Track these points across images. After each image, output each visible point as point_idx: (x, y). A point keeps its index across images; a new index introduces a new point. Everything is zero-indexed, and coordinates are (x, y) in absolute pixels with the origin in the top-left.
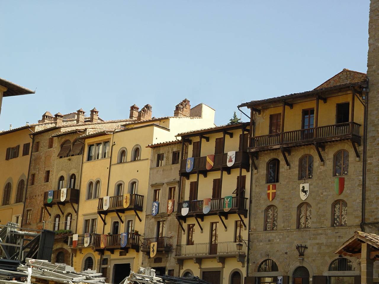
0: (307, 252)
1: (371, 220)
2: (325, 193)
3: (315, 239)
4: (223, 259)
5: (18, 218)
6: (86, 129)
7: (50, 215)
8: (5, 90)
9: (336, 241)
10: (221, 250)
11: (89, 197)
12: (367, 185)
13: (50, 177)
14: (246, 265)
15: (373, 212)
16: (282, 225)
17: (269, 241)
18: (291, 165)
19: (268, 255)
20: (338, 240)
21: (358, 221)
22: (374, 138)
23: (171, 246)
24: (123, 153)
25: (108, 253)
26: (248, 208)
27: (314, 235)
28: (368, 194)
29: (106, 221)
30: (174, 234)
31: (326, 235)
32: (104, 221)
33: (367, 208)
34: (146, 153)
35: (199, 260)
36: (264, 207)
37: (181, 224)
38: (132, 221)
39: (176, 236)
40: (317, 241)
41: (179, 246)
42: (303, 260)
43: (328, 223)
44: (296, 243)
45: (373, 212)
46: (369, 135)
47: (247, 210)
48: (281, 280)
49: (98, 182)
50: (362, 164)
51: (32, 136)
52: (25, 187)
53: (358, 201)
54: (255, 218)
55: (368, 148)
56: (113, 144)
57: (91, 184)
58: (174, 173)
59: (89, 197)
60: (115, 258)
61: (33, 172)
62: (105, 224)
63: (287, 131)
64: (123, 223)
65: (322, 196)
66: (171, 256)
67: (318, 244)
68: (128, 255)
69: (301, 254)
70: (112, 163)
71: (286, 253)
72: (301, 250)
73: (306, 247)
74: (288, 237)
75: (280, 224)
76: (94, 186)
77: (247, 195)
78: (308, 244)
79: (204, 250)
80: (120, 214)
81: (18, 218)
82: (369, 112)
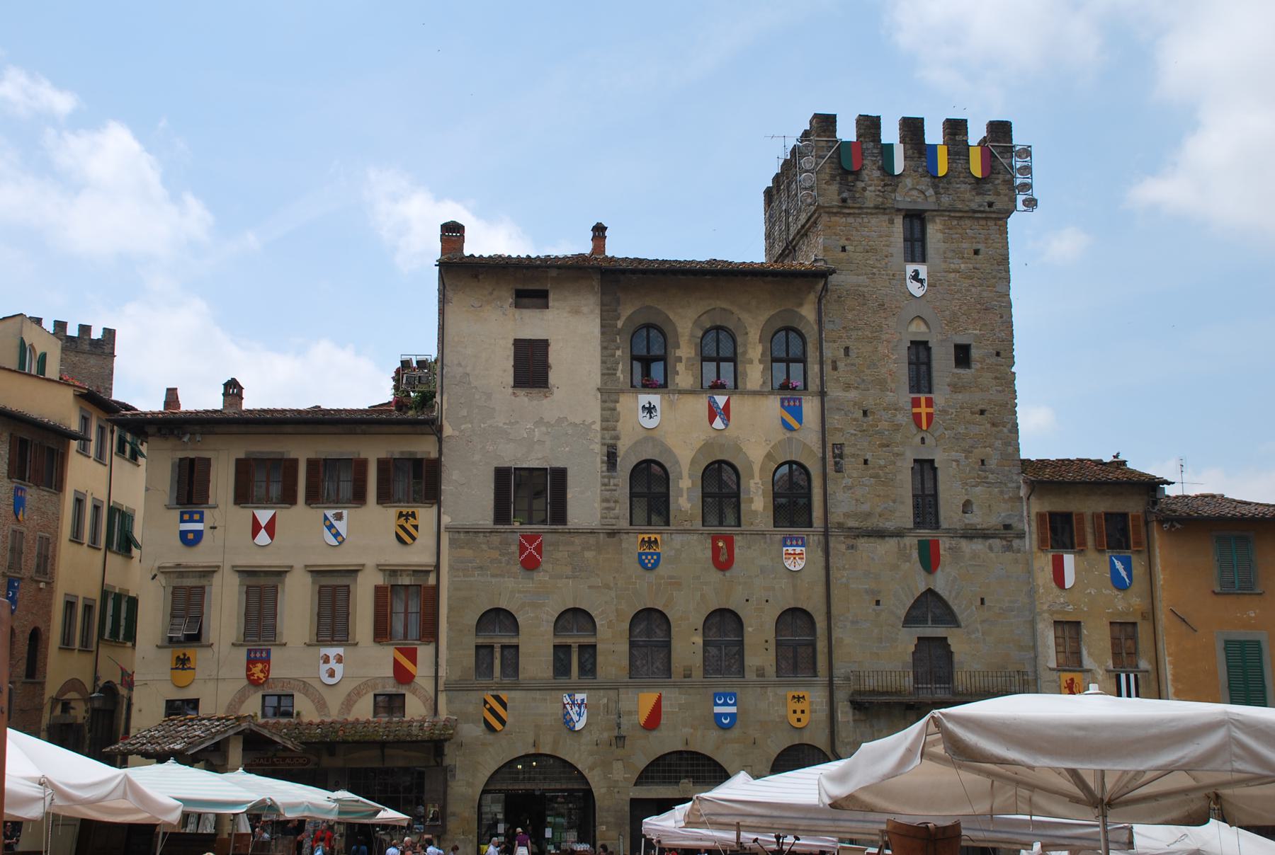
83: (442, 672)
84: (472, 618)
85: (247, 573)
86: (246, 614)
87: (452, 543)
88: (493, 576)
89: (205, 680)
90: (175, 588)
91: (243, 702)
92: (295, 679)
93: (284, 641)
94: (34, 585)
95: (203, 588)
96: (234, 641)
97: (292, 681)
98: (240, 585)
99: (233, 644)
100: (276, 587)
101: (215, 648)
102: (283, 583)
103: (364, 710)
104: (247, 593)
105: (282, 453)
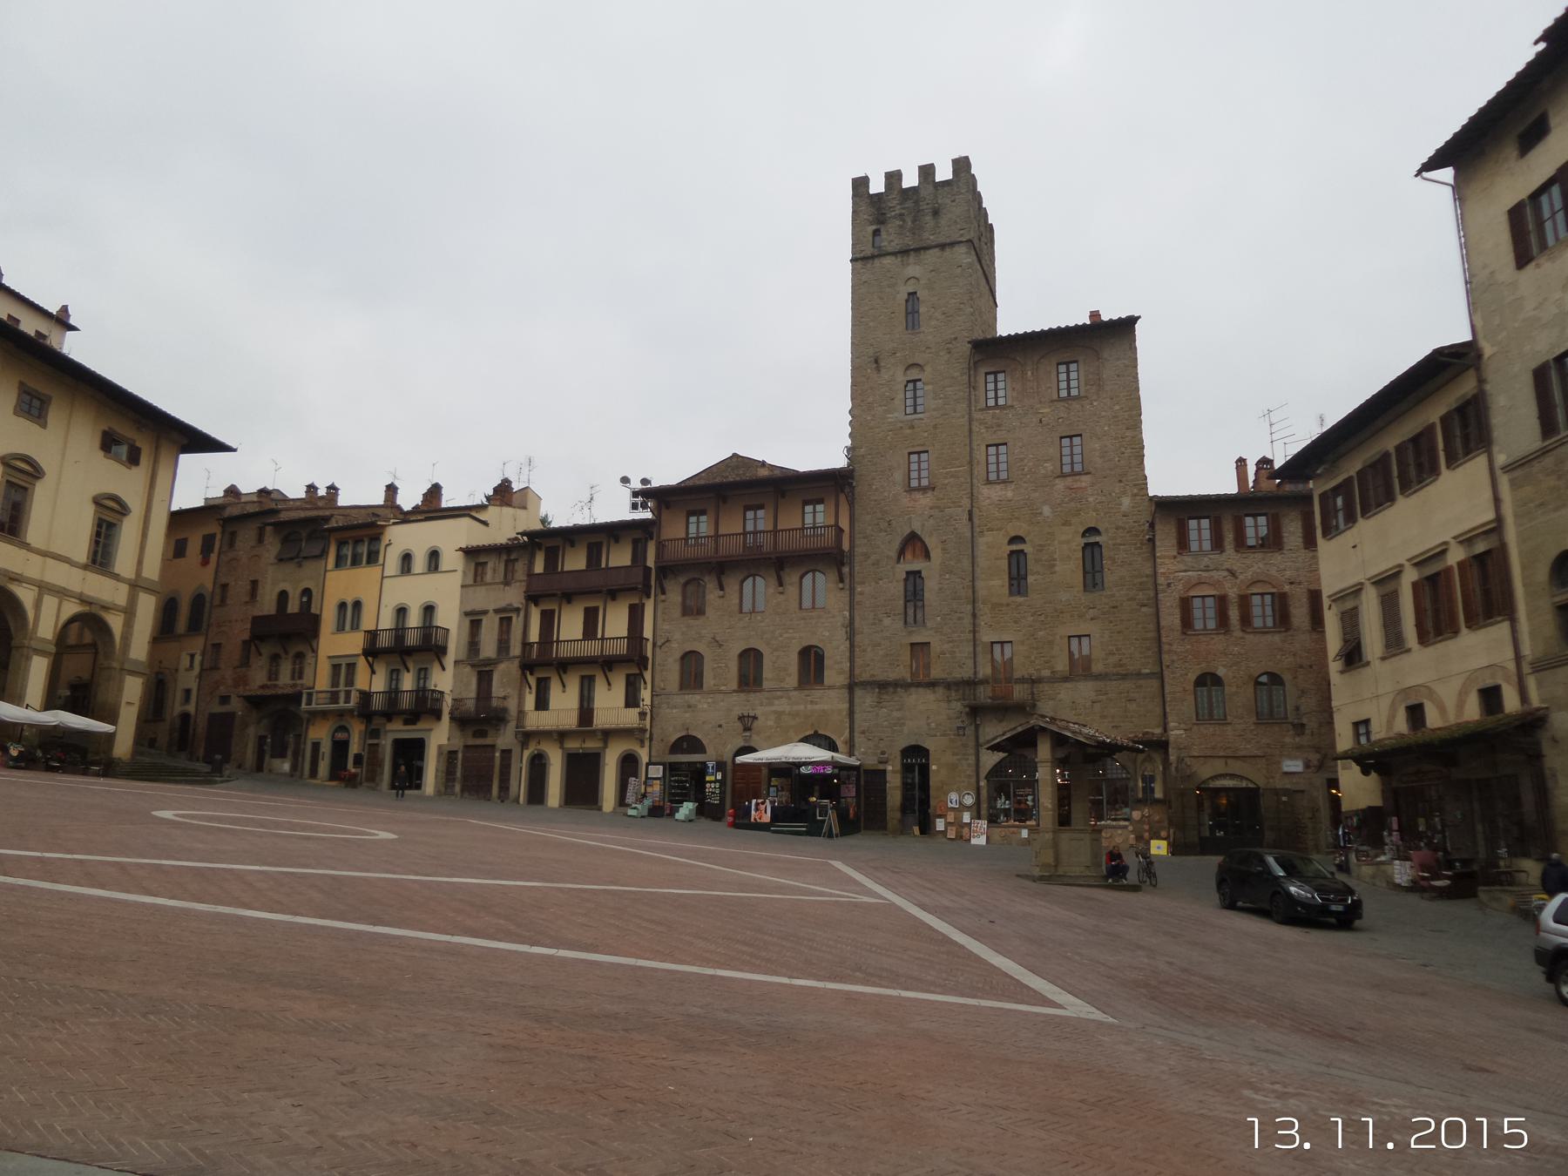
0: (756, 723)
1: (865, 677)
2: (785, 635)
3: (772, 704)
4: (608, 735)
5: (192, 656)
6: (332, 516)
7: (260, 655)
8: (185, 442)
9: (806, 707)
10: (602, 719)
11: (340, 628)
12: (857, 625)
13: (260, 591)
14: (647, 743)
15: (868, 665)
16: (712, 682)
17: (689, 706)
18: (727, 589)
19: (688, 729)
20: (809, 707)
21: (842, 680)
22: (866, 556)
23: (505, 710)
24: (407, 558)
25: (377, 721)
26: (649, 654)
27: (767, 698)
28: (858, 638)
29: (376, 667)
30: (512, 692)
31: (789, 698)
32: (371, 666)
33: (858, 661)
34: (452, 559)
35: (561, 736)
36: (678, 655)
37: (524, 675)
38: (426, 669)
39: (516, 696)
40: (774, 708)
41: (521, 713)
42: (750, 736)
43: (792, 681)
44: (737, 712)
45: (868, 665)
46: (858, 550)
47: (647, 659)
48: (713, 767)
49: (357, 605)
50: (848, 592)
51: (221, 522)
52: (208, 605)
53: (842, 648)
54: (662, 671)
55: (856, 568)
56: (388, 543)
57: (342, 606)
58: (514, 596)
59: (340, 628)
60: (397, 730)
61: (223, 580)
62: (373, 672)
63: (668, 538)
64: (408, 671)
65: (780, 639)
66: (505, 730)
67: (775, 712)
68: (420, 725)
69: (747, 729)
70: (385, 575)
71: (720, 726)
72: (747, 723)
73: (755, 718)
74: (723, 701)
75: (709, 680)
76: (350, 612)
77: (648, 633)
78: (759, 712)
79: (570, 720)
80: (406, 658)
81: (192, 656)
82: (856, 516)
83: (1526, 650)
84: (1542, 573)
85: (1379, 582)
87: (1514, 485)
88: (1557, 509)
89: (1371, 699)
90: (1342, 613)
99: (1383, 659)
101: (1372, 664)
103: (1473, 711)
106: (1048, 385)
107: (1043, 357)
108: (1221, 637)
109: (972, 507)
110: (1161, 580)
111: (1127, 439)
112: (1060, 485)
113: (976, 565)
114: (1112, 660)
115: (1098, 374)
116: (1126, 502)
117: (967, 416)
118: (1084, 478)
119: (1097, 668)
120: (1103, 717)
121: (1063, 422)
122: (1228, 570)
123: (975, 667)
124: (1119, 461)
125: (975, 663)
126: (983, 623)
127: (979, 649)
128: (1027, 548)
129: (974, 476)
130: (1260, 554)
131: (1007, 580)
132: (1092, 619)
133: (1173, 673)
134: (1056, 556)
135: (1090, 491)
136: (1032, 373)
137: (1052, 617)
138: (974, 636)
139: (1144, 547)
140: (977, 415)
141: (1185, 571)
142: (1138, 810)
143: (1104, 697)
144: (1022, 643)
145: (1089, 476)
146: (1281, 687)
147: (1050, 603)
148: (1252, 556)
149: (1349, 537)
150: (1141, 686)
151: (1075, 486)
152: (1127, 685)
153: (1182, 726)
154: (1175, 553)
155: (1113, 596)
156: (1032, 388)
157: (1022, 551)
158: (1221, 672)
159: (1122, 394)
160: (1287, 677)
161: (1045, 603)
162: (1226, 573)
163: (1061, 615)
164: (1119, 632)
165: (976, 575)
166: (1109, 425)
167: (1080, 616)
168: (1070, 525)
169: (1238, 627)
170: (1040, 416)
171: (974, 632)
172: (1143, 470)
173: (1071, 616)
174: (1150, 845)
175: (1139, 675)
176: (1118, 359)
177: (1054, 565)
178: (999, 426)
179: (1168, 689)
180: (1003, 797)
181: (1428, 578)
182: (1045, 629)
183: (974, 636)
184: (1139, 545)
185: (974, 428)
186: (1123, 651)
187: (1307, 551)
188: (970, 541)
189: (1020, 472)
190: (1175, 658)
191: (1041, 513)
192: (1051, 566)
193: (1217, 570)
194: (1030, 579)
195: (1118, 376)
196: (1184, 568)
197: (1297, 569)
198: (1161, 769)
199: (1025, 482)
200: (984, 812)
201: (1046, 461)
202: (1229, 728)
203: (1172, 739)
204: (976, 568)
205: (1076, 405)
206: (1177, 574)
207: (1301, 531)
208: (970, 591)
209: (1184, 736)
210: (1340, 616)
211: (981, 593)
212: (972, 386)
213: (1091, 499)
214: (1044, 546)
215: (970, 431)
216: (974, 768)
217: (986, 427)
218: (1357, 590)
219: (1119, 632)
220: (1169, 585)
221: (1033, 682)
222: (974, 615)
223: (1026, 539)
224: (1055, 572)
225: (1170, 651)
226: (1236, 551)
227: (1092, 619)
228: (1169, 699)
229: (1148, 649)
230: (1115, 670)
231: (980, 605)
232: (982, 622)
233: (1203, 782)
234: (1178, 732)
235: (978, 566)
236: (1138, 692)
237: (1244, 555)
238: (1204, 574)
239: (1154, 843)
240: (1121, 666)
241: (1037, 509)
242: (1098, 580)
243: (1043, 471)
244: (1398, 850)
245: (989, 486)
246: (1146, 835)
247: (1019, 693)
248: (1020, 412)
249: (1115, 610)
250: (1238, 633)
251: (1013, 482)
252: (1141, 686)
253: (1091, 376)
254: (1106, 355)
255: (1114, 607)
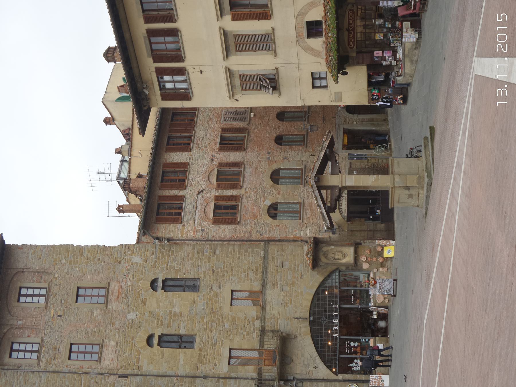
85: (227, 52)
86: (255, 50)
89: (299, 70)
90: (242, 89)
91: (313, 48)
92: (296, 21)
93: (271, 29)
94: (252, 122)
95: (240, 75)
96: (273, 57)
97: (298, 22)
98: (236, 55)
99: (276, 56)
100: (235, 36)
101: (277, 66)
102: (231, 32)
104: (240, 51)
105: (145, 38)
106: (33, 309)
107: (10, 313)
108: (244, 201)
109: (117, 374)
110: (199, 235)
111: (89, 256)
112: (113, 305)
113: (164, 374)
114: (252, 275)
115: (35, 272)
116: (137, 259)
117: (41, 374)
118: (111, 287)
119: (257, 286)
120: (293, 284)
121: (65, 300)
122: (198, 194)
123: (248, 379)
124: (104, 262)
125: (244, 379)
126: (213, 371)
127: (233, 375)
128: (158, 333)
129: (92, 371)
130: (190, 176)
131: (180, 350)
132: (220, 288)
133: (266, 232)
134: (168, 311)
135: (123, 284)
136: (20, 320)
137: (215, 317)
138: (222, 378)
139: (172, 249)
140: (42, 366)
141: (195, 220)
142: (362, 265)
143: (279, 283)
144: (232, 340)
145: (111, 284)
146: (281, 171)
147: (203, 318)
148: (190, 180)
149: (194, 76)
150: (273, 258)
151: (117, 294)
152: (271, 266)
153: (304, 228)
154: (180, 226)
155: (205, 273)
156: (32, 321)
157: (160, 337)
158: (268, 203)
159: (55, 257)
160: (275, 167)
161: (203, 321)
162: (200, 196)
163: (214, 310)
164: (232, 270)
165: (173, 374)
166: (76, 267)
167: (217, 295)
168: (146, 299)
169: (238, 190)
170: (56, 316)
171: (219, 378)
172: (115, 247)
173: (216, 303)
174: (387, 258)
175: (265, 258)
176: (28, 257)
177: (175, 313)
178: (55, 348)
179: (277, 236)
180: (351, 365)
181: (231, 9)
182: (223, 322)
183: (222, 378)
184: (170, 253)
185: (51, 369)
186: (246, 267)
187: (192, 151)
188: (143, 378)
189: (97, 335)
190: (255, 230)
191: (132, 321)
192: (174, 316)
193: (197, 201)
194: (183, 332)
195: (40, 258)
196: (192, 220)
197: (204, 156)
198: (333, 247)
199: (105, 331)
200: (363, 377)
201: (92, 314)
202: (307, 201)
203: (312, 235)
204: (167, 374)
205: (54, 290)
206: (196, 225)
207: (178, 153)
208: (185, 380)
209: (310, 228)
210: (243, 92)
211: (188, 371)
212: (18, 368)
213: (129, 284)
214: (158, 320)
215: (54, 372)
216: (329, 383)
217: (54, 359)
218: (230, 73)
219: (232, 270)
220: (203, 230)
221: (263, 331)
222: (205, 377)
223: (151, 333)
224: (181, 313)
225: (251, 233)
226: (185, 189)
227: (220, 288)
228: (284, 235)
229: (246, 251)
230: (260, 274)
231: (198, 373)
232: (211, 372)
233: (344, 219)
234: (308, 231)
235: (166, 372)
236: (277, 259)
237: (189, 185)
238: (199, 208)
239: (386, 255)
240: (257, 270)
241: (129, 324)
242: (191, 283)
243: (100, 317)
244: (396, 40)
245: (102, 360)
246: (380, 260)
247: (271, 344)
248: (48, 331)
249: (215, 271)
250: (242, 192)
251: (103, 340)
252: (273, 258)
253: (34, 279)
254: (21, 266)
255: (213, 272)
